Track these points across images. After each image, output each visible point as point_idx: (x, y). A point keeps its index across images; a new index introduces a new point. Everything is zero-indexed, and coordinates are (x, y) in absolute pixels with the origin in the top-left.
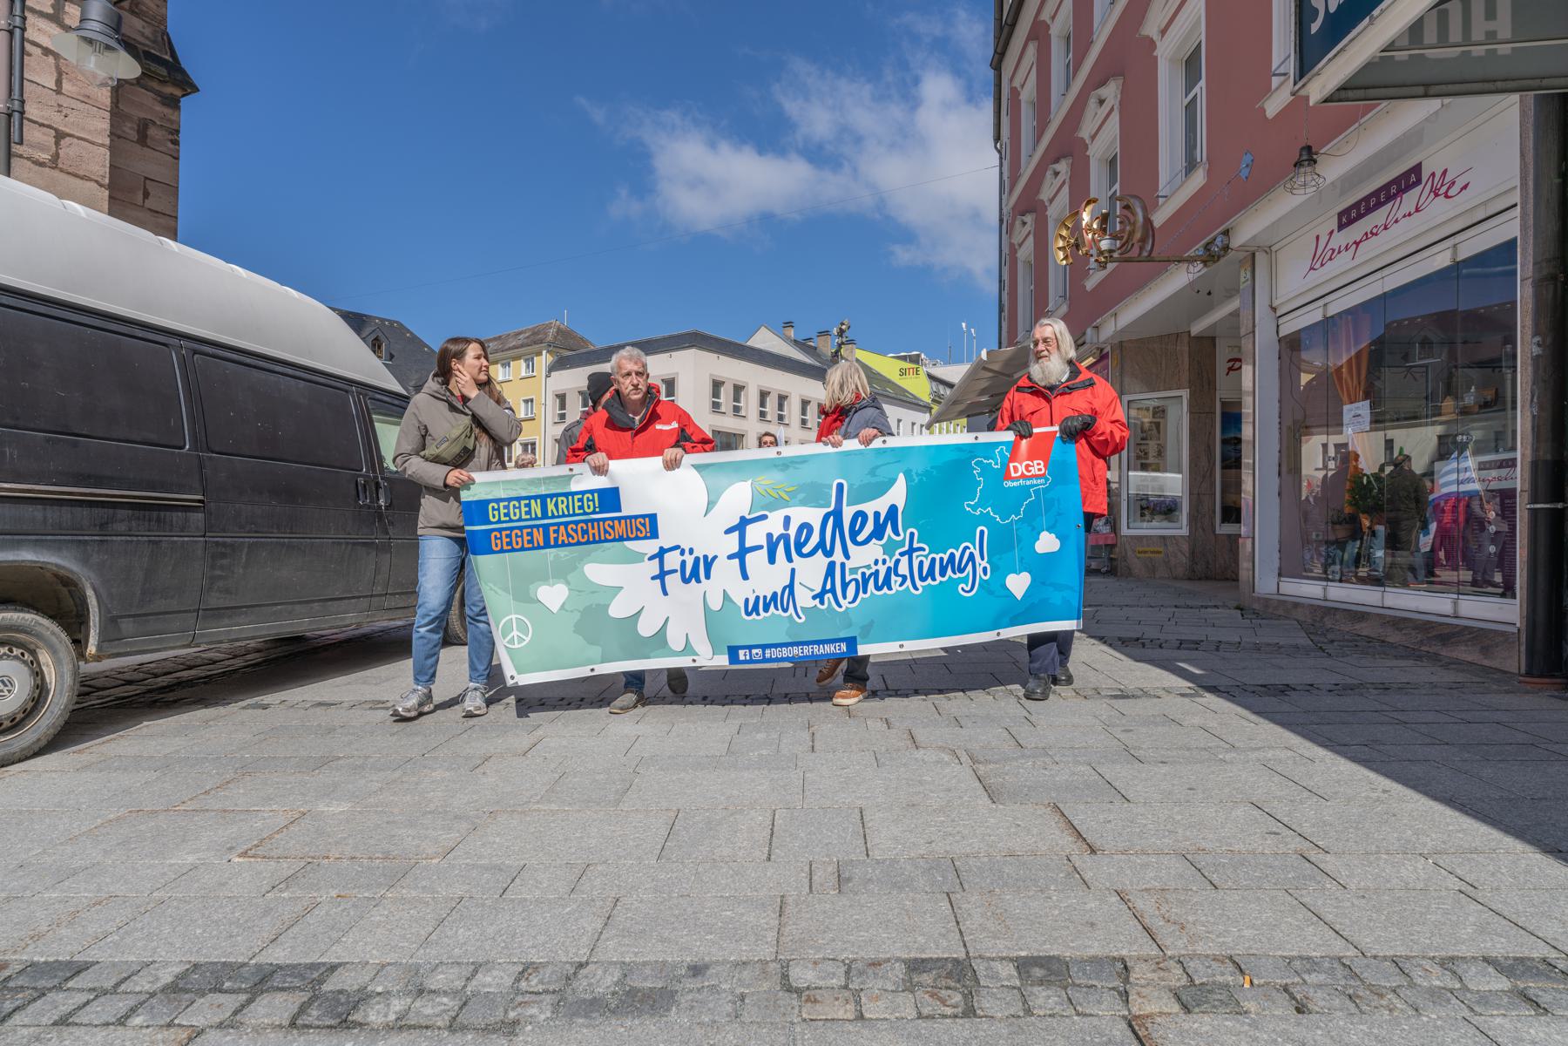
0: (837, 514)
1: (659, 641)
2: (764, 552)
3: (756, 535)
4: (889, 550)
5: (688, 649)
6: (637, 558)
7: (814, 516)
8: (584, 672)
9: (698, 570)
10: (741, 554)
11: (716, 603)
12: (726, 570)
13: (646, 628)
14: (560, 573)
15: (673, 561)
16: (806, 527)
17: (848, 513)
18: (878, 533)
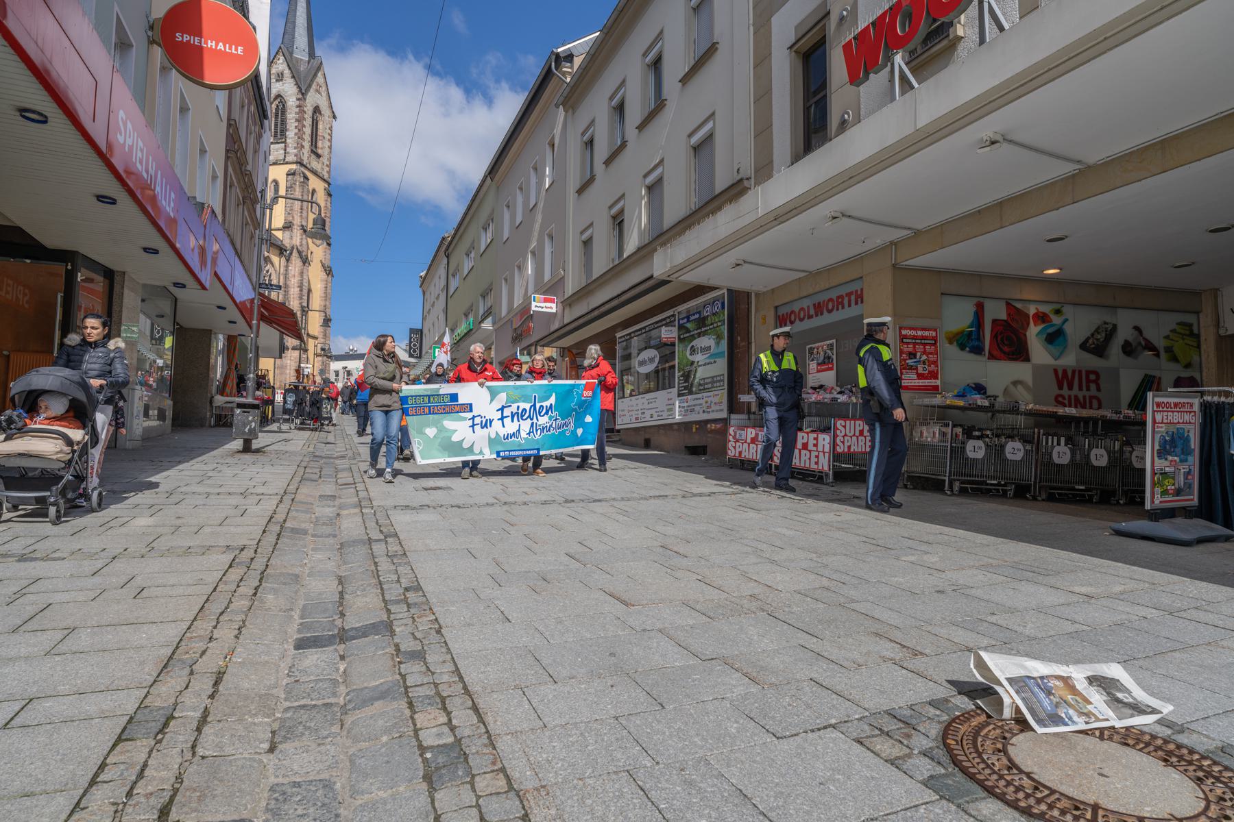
0: (534, 405)
1: (470, 450)
3: (507, 412)
4: (550, 418)
5: (481, 453)
6: (465, 419)
7: (527, 406)
9: (487, 424)
10: (502, 419)
11: (493, 436)
12: (497, 424)
13: (466, 445)
14: (436, 424)
15: (477, 420)
17: (538, 405)
18: (547, 413)
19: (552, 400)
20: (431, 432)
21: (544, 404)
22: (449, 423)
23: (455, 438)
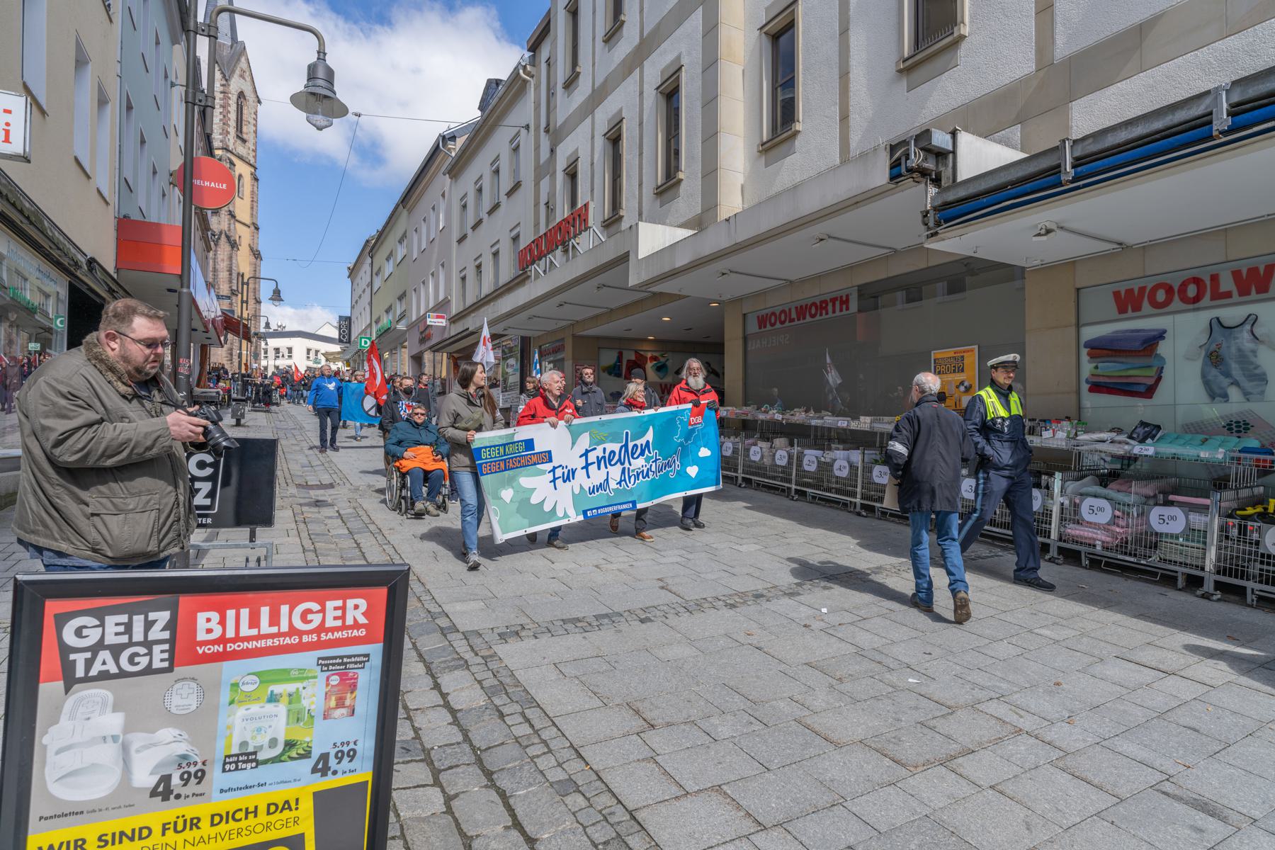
0: (626, 445)
2: (595, 466)
4: (647, 460)
5: (566, 516)
8: (521, 533)
9: (570, 476)
10: (586, 467)
11: (577, 491)
12: (580, 474)
13: (547, 507)
15: (559, 472)
16: (613, 452)
17: (631, 445)
18: (642, 454)
19: (649, 436)
20: (507, 494)
21: (638, 442)
22: (525, 481)
23: (535, 500)
